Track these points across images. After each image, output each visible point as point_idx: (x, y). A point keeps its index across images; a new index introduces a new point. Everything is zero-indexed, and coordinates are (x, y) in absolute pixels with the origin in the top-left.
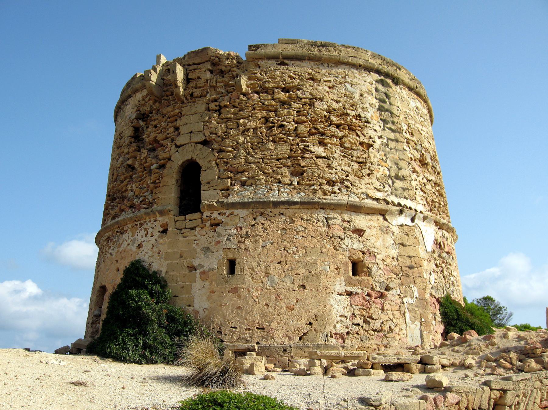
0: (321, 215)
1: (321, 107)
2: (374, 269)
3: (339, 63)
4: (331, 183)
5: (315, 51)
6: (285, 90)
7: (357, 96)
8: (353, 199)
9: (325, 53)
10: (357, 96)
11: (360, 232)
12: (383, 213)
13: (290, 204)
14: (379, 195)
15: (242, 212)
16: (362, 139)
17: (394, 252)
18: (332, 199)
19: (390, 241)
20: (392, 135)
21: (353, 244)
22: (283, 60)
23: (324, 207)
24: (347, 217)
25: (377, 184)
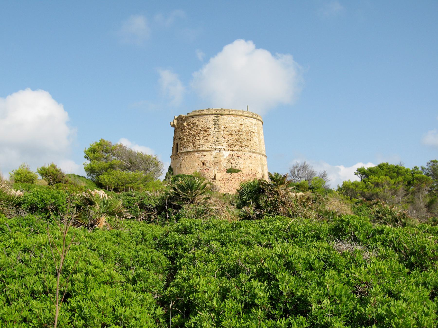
0: (196, 153)
1: (199, 127)
2: (207, 164)
3: (204, 115)
4: (199, 145)
5: (199, 113)
6: (193, 124)
7: (208, 122)
8: (204, 149)
9: (202, 113)
10: (208, 122)
11: (205, 156)
12: (210, 151)
13: (190, 152)
14: (210, 147)
15: (183, 154)
16: (208, 133)
17: (213, 160)
18: (199, 149)
19: (212, 157)
20: (217, 130)
21: (203, 159)
22: (192, 117)
23: (197, 151)
24: (202, 153)
25: (210, 144)
